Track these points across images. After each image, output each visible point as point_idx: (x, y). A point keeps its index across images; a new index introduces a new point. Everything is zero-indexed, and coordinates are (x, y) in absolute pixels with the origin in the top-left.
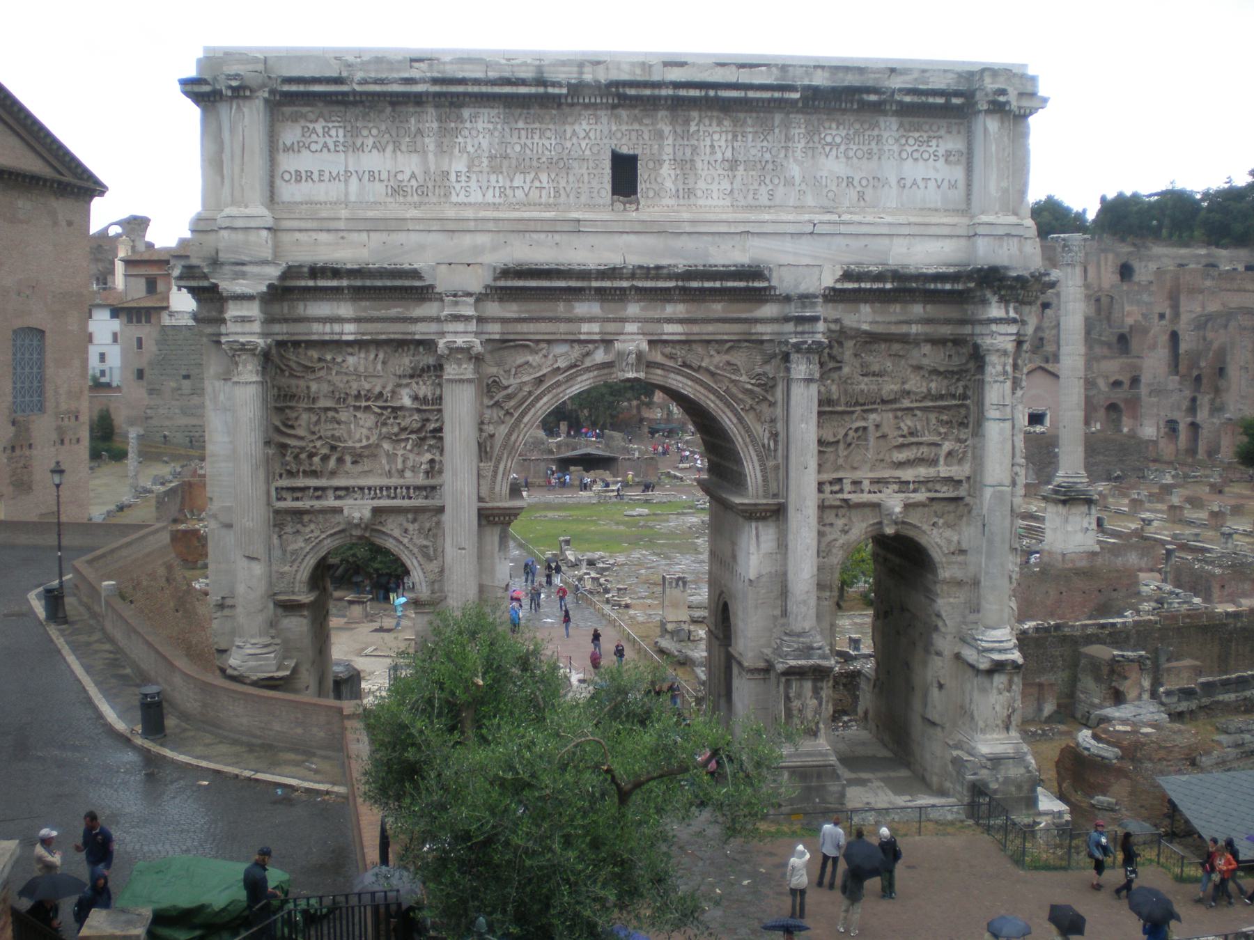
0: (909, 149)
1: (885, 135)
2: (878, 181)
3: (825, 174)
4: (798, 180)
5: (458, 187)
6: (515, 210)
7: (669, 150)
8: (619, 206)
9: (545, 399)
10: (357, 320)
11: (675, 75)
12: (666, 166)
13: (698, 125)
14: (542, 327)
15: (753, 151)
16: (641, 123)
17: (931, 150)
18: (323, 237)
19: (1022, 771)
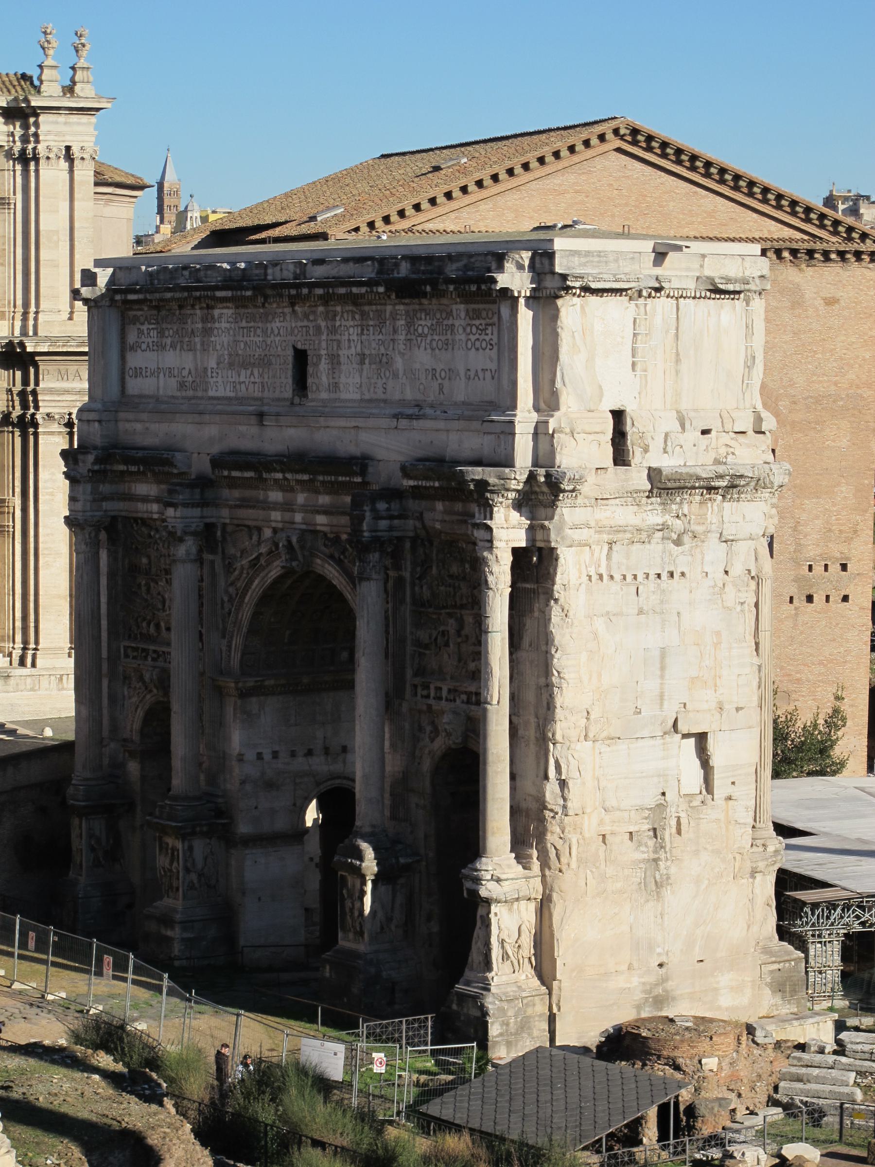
0: (473, 338)
1: (457, 323)
2: (451, 373)
3: (417, 366)
4: (401, 373)
5: (212, 381)
6: (241, 404)
7: (324, 344)
8: (297, 400)
9: (256, 582)
10: (158, 500)
11: (318, 272)
12: (323, 360)
13: (340, 320)
14: (251, 513)
15: (374, 345)
16: (308, 320)
17: (487, 338)
18: (138, 426)
19: (478, 1014)
